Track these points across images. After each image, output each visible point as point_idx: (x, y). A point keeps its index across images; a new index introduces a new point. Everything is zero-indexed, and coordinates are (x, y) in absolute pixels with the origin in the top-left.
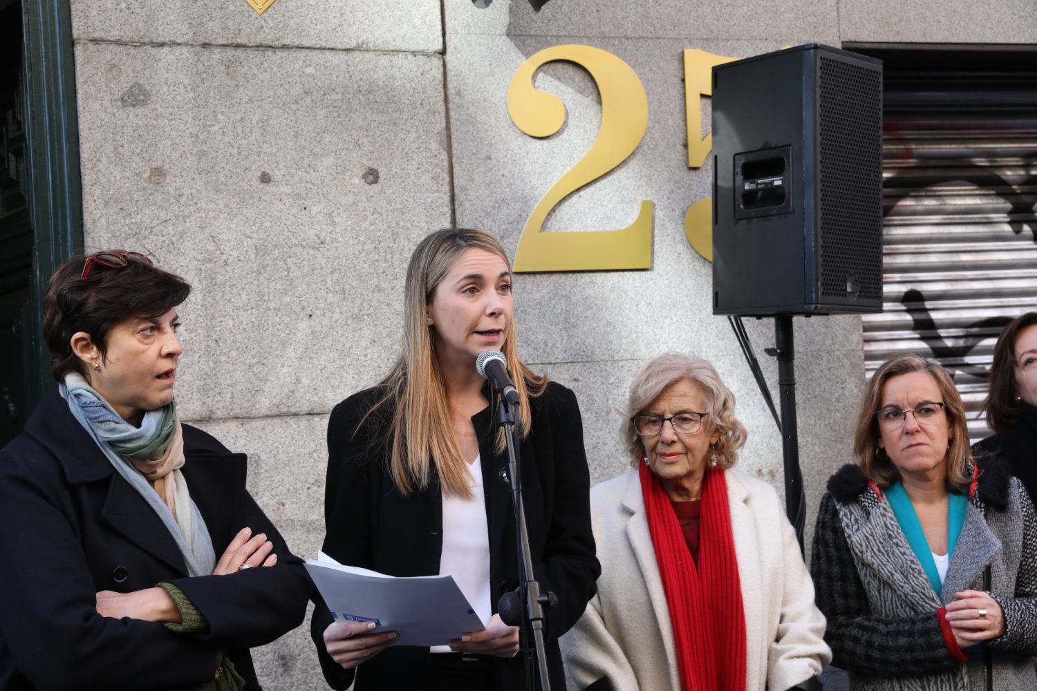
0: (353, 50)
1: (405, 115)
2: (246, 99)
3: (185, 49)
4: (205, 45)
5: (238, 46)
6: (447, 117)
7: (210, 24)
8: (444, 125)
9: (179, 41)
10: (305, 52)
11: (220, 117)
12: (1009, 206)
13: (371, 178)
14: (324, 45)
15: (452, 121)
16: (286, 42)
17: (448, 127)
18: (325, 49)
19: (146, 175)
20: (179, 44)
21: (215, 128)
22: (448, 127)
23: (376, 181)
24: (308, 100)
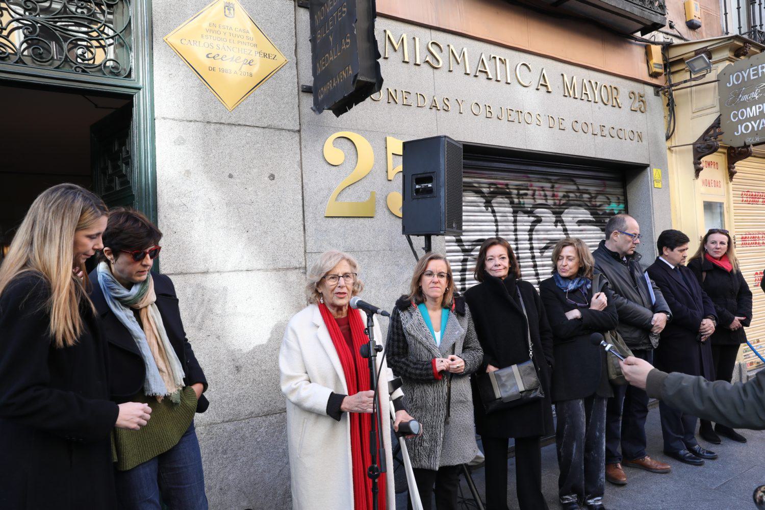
0: (266, 128)
1: (285, 154)
2: (224, 144)
3: (200, 124)
4: (208, 122)
5: (221, 123)
6: (301, 156)
7: (210, 114)
8: (300, 159)
9: (198, 120)
10: (247, 127)
11: (213, 151)
12: (484, 201)
13: (272, 178)
14: (255, 125)
15: (303, 157)
16: (240, 123)
17: (301, 160)
18: (255, 127)
19: (183, 173)
20: (198, 121)
21: (211, 155)
22: (301, 160)
23: (273, 179)
24: (248, 146)
